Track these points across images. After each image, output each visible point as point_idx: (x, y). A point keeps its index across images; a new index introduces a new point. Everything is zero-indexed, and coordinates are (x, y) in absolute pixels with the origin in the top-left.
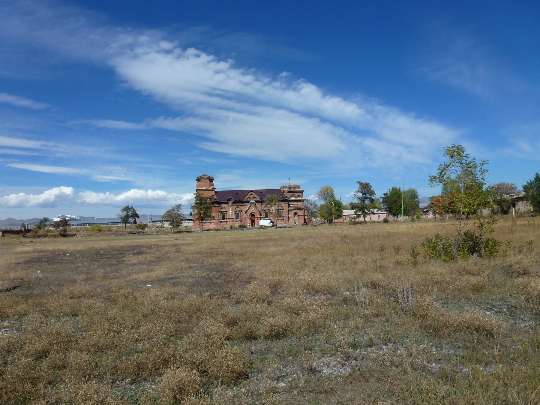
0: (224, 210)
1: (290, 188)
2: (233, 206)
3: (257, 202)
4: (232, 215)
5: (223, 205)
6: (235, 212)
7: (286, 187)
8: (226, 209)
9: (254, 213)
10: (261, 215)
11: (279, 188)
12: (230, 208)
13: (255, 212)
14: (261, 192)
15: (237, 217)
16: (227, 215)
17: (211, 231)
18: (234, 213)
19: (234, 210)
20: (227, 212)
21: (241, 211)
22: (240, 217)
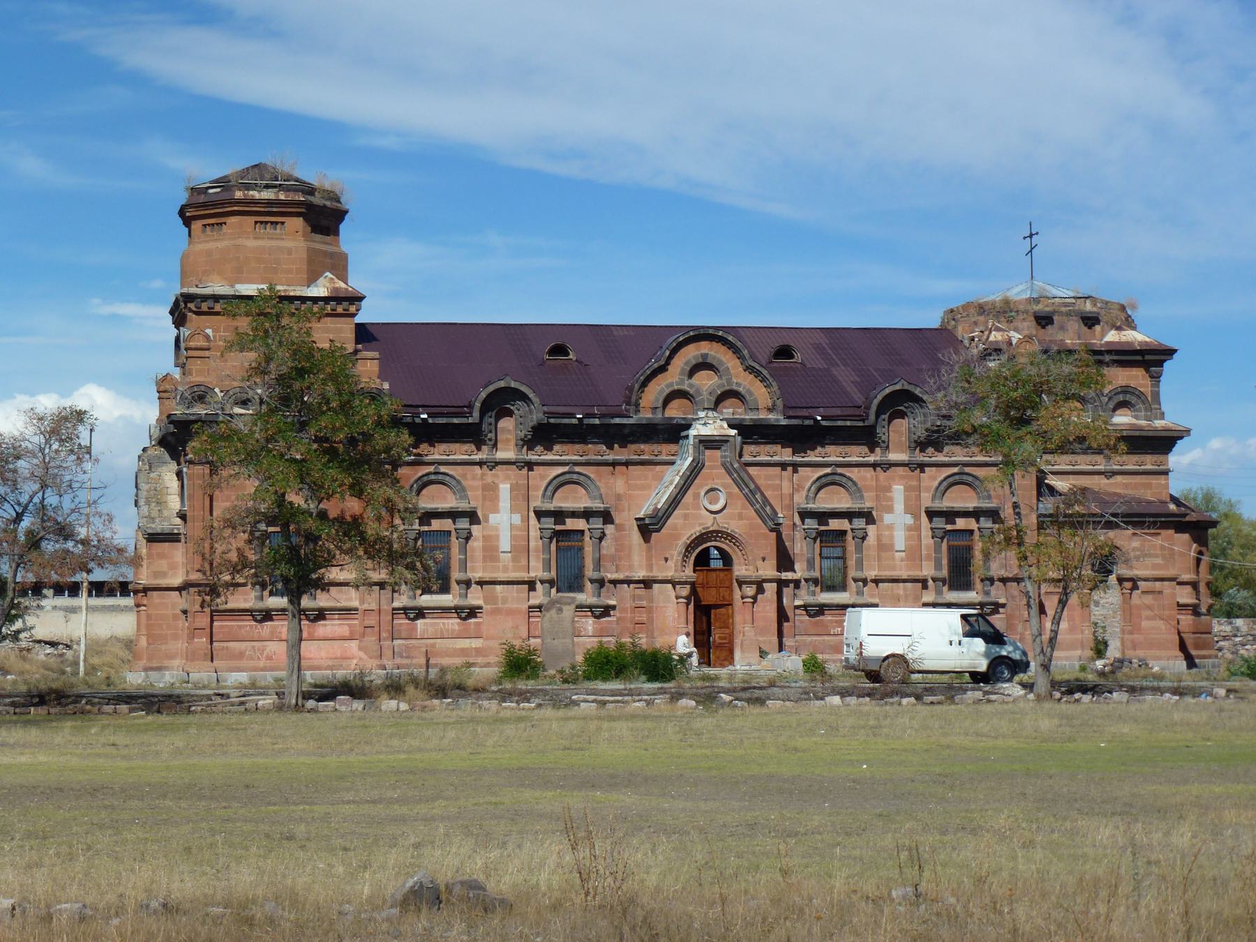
1: (1044, 320)
2: (530, 465)
3: (752, 432)
4: (521, 549)
5: (438, 452)
6: (549, 523)
7: (1005, 311)
8: (461, 491)
9: (730, 537)
10: (785, 560)
11: (930, 319)
12: (505, 489)
13: (733, 526)
14: (784, 352)
15: (569, 580)
16: (476, 544)
17: (389, 704)
18: (534, 533)
19: (537, 503)
20: (473, 517)
21: (607, 517)
22: (589, 572)
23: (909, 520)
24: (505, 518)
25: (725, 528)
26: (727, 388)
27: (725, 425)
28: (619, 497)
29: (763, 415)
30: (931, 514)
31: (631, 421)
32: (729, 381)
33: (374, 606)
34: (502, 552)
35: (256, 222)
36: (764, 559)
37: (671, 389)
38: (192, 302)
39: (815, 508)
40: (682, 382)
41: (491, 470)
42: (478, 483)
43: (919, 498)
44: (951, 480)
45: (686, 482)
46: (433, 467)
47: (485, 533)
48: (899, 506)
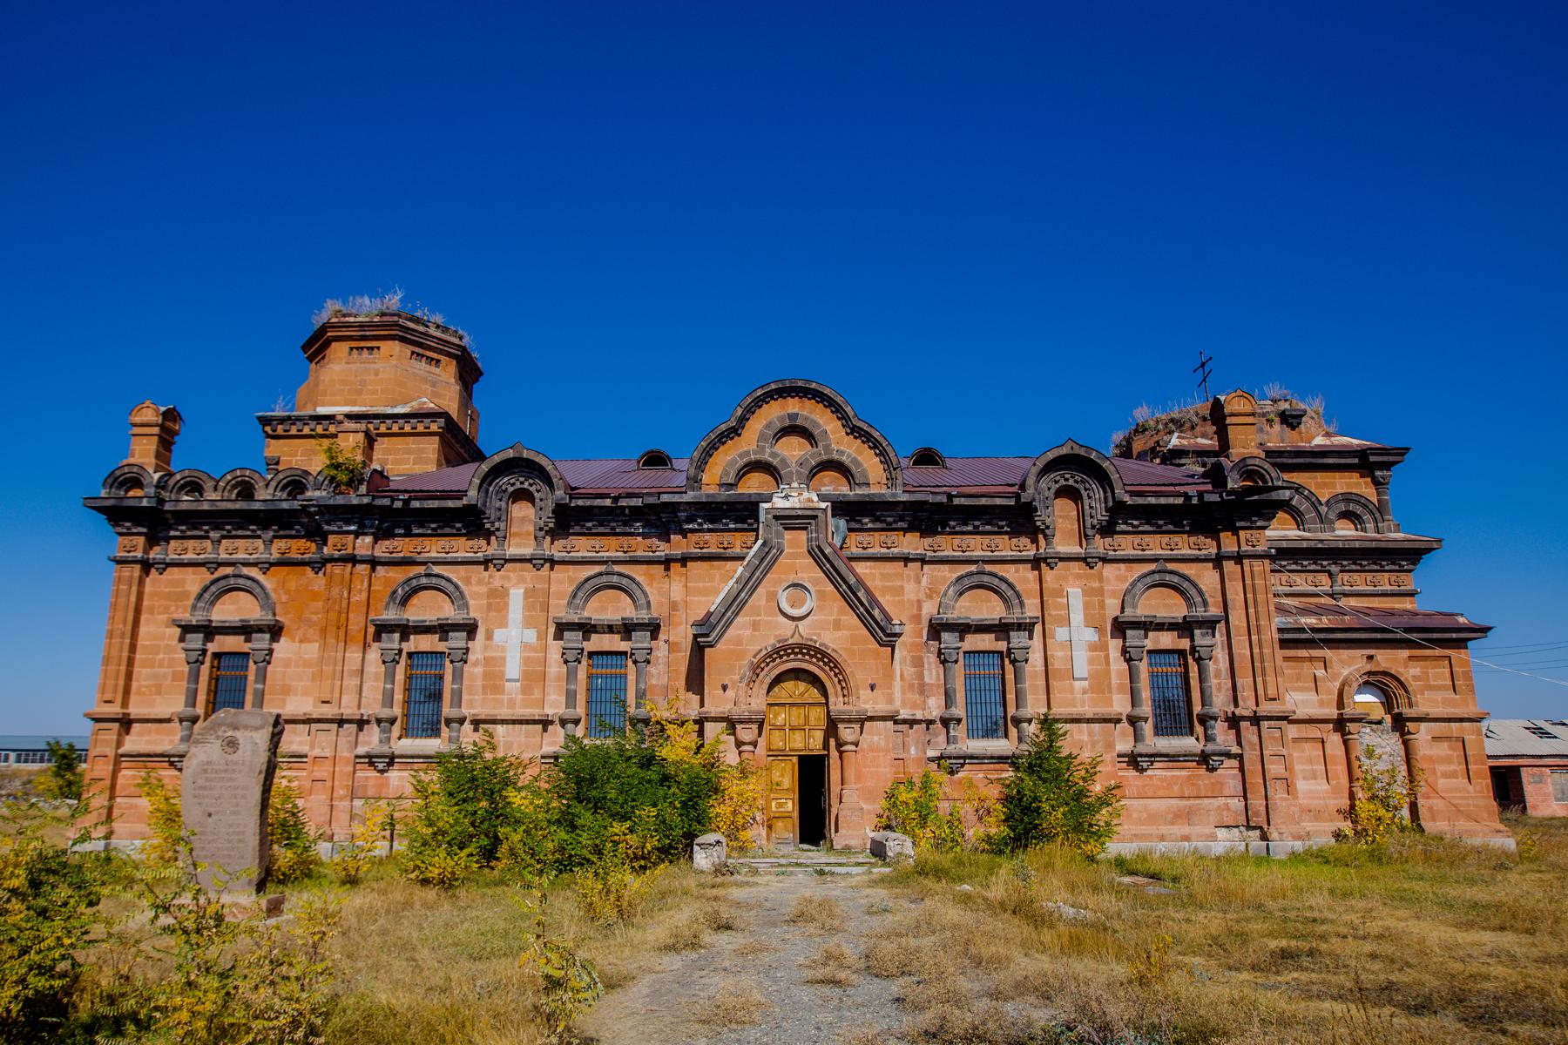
0: (446, 611)
3: (853, 511)
4: (534, 677)
5: (434, 548)
12: (516, 596)
16: (474, 671)
23: (1091, 635)
24: (513, 633)
25: (811, 640)
26: (824, 457)
27: (815, 498)
28: (674, 606)
29: (874, 490)
30: (1120, 628)
31: (689, 497)
32: (827, 449)
33: (328, 753)
34: (508, 680)
35: (352, 349)
36: (872, 687)
37: (745, 460)
38: (269, 425)
39: (953, 619)
40: (762, 450)
41: (499, 570)
42: (483, 589)
43: (1102, 605)
44: (1149, 580)
45: (752, 574)
46: (424, 567)
47: (487, 655)
48: (1077, 617)
